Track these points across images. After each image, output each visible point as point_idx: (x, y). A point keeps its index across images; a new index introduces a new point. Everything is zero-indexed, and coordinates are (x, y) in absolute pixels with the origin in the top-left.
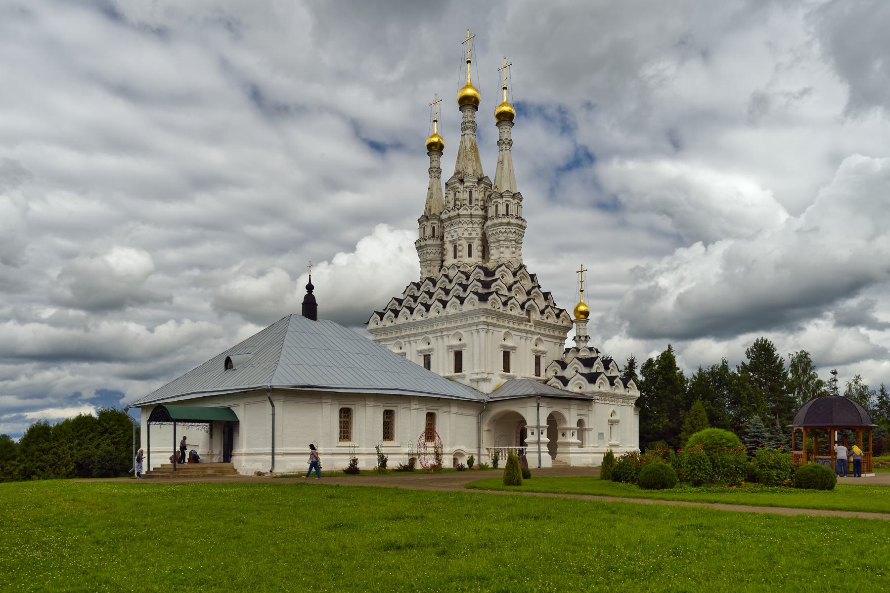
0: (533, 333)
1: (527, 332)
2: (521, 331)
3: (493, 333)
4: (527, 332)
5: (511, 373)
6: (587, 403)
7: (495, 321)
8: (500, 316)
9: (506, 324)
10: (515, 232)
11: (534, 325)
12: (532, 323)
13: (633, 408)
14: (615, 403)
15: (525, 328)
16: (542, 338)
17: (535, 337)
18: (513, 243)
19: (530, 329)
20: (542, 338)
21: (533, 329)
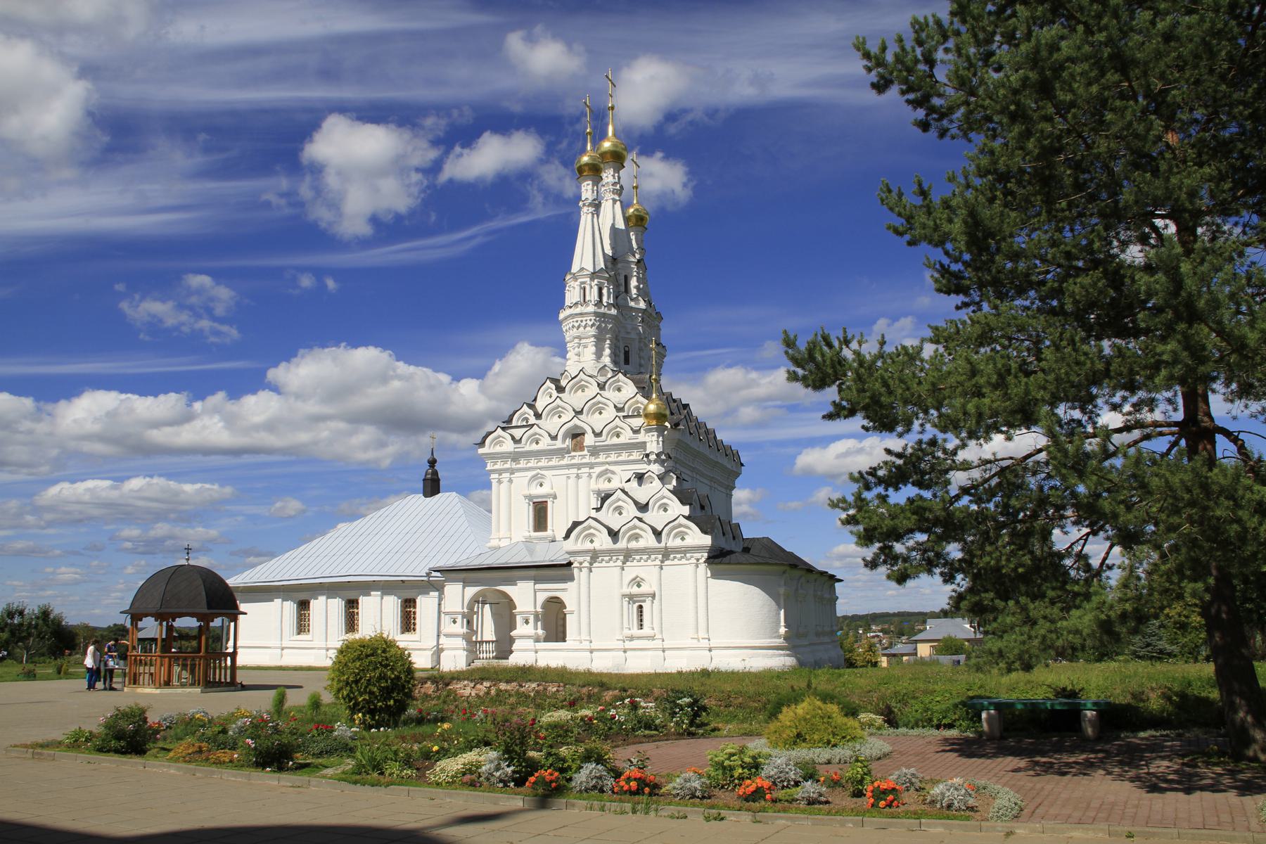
0: (591, 466)
1: (579, 466)
2: (569, 466)
3: (510, 481)
4: (579, 466)
5: (549, 533)
7: (507, 466)
8: (515, 457)
9: (532, 463)
10: (573, 326)
12: (585, 452)
13: (703, 567)
14: (642, 563)
16: (611, 468)
17: (598, 470)
18: (576, 341)
19: (584, 461)
20: (611, 468)
21: (586, 460)
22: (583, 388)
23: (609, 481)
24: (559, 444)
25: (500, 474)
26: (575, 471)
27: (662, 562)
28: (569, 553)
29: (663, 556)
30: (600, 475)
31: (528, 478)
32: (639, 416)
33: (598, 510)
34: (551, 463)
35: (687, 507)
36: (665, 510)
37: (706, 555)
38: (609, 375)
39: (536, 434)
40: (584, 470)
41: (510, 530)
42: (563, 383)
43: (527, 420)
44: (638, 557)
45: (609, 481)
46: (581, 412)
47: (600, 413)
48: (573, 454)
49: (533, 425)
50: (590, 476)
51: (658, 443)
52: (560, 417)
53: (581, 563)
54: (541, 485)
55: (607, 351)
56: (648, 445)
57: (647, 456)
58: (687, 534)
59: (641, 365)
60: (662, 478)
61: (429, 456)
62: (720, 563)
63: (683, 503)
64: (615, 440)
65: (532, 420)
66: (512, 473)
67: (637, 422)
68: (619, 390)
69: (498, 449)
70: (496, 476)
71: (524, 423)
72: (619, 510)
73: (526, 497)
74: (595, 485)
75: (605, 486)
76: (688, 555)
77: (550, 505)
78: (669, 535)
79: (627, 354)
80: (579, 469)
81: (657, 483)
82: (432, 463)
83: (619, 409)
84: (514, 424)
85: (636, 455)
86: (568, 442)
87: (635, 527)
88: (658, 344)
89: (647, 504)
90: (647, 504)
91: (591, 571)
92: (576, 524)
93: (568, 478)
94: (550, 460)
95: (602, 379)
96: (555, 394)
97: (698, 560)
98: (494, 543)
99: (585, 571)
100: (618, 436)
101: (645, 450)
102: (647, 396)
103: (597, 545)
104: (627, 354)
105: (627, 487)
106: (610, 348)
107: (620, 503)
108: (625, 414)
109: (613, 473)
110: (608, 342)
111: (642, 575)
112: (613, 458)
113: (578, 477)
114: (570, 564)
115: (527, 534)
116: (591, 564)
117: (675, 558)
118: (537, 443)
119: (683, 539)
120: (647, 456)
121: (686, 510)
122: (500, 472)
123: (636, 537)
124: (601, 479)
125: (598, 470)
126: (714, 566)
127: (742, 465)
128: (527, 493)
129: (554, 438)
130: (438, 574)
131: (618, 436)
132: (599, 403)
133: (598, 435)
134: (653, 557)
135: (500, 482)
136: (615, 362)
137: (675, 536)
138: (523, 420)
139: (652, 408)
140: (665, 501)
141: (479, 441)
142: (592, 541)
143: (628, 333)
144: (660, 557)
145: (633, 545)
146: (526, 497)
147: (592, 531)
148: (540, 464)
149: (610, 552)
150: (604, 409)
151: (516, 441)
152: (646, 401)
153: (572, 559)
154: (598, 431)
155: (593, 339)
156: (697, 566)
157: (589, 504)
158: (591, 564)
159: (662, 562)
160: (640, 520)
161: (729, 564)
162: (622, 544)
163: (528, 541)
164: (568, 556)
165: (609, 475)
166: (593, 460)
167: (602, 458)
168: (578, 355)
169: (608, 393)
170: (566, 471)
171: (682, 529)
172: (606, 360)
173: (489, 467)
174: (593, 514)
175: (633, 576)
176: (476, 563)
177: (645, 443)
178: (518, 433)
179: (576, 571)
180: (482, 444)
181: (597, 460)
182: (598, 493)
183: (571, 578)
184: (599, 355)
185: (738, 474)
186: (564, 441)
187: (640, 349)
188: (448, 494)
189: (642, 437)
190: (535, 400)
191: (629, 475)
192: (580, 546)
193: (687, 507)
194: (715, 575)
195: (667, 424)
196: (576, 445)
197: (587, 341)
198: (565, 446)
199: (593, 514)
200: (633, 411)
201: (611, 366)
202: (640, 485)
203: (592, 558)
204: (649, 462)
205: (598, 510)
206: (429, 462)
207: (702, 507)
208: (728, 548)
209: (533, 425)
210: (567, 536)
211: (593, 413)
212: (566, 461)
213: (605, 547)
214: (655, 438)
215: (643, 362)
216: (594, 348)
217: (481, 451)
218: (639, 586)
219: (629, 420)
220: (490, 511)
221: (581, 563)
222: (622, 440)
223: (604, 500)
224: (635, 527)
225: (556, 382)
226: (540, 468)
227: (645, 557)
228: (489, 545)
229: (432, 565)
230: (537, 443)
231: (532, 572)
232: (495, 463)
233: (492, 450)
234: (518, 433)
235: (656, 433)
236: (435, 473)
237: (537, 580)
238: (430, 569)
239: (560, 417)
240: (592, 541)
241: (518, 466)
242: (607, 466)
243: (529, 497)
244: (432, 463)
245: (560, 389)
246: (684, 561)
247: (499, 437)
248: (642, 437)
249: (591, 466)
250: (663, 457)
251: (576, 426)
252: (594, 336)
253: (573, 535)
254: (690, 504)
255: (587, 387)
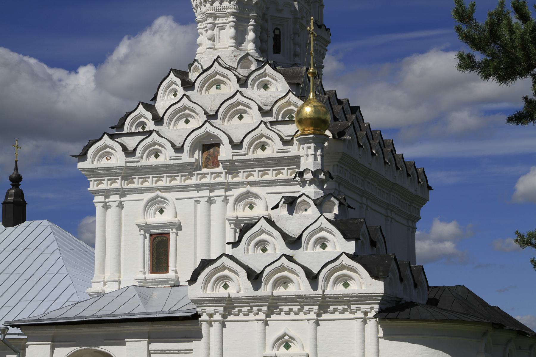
0: (228, 187)
1: (211, 187)
3: (121, 206)
4: (211, 187)
5: (171, 274)
6: (188, 327)
11: (224, 171)
12: (220, 169)
13: (372, 324)
14: (292, 316)
15: (204, 181)
16: (254, 190)
17: (236, 192)
18: (210, 20)
19: (219, 180)
20: (254, 190)
22: (218, 84)
23: (251, 207)
24: (185, 158)
25: (107, 197)
26: (206, 193)
27: (319, 315)
28: (195, 301)
29: (320, 308)
30: (239, 200)
31: (143, 203)
32: (291, 121)
33: (235, 244)
34: (174, 183)
35: (352, 244)
36: (324, 246)
37: (377, 307)
38: (253, 68)
39: (155, 144)
40: (217, 192)
41: (119, 270)
42: (192, 76)
43: (143, 125)
44: (286, 308)
45: (251, 207)
46: (214, 116)
47: (241, 118)
48: (204, 171)
49: (150, 133)
50: (226, 200)
51: (315, 158)
52: (187, 122)
53: (211, 316)
54: (161, 211)
55: (251, 35)
56: (302, 160)
57: (301, 174)
58: (351, 278)
59: (295, 55)
60: (320, 204)
61: (11, 171)
62: (396, 319)
63: (347, 237)
64: (260, 154)
65: (150, 125)
66: (123, 195)
67: (289, 130)
68: (266, 87)
69: (104, 163)
70: (101, 199)
71: (140, 130)
72: (263, 246)
73: (140, 227)
74: (230, 213)
75: (244, 213)
76: (353, 307)
77: (172, 237)
78: (327, 279)
79: (277, 39)
80: (211, 191)
81: (313, 211)
82: (16, 180)
83: (264, 113)
84: (126, 130)
85: (286, 174)
86: (197, 155)
87: (283, 268)
88: (319, 26)
89: (300, 237)
90: (300, 237)
91: (223, 325)
92: (205, 263)
93: (197, 202)
94: (174, 178)
95: (243, 72)
96: (181, 91)
97: (366, 313)
98: (97, 288)
99: (216, 325)
100: (263, 148)
101: (299, 166)
102: (303, 96)
103: (232, 291)
104: (277, 39)
105: (274, 215)
106: (254, 31)
107: (264, 236)
108: (273, 119)
109: (256, 196)
110: (252, 22)
111: (292, 333)
112: (256, 176)
113: (210, 201)
114: (196, 316)
115: (142, 276)
116: (224, 316)
117: (335, 310)
118: (157, 156)
119: (346, 285)
120: (301, 174)
121: (351, 247)
122: (107, 193)
123: (285, 282)
124: (241, 205)
125: (236, 192)
126: (387, 322)
127: (430, 188)
128: (142, 221)
129: (179, 149)
130: (18, 330)
131: (263, 148)
132: (239, 103)
133: (236, 146)
134: (306, 308)
135: (106, 207)
136: (260, 49)
137: (336, 282)
138: (138, 126)
139: (308, 110)
140: (323, 234)
141: (79, 152)
142: (226, 287)
143: (280, 11)
144: (316, 308)
145: (281, 291)
146: (140, 227)
147: (226, 272)
148: (160, 184)
149: (249, 301)
150: (245, 112)
151: (129, 153)
152: (300, 102)
153: (199, 310)
154: (236, 140)
155: (231, 18)
156: (365, 322)
157: (224, 236)
158: (224, 316)
159: (319, 315)
160: (290, 258)
161: (408, 319)
162: (266, 290)
163: (143, 285)
164: (193, 306)
165: (252, 199)
166: (230, 179)
167: (241, 177)
168: (212, 39)
169: (251, 92)
170: (195, 194)
171: (345, 272)
172: (250, 46)
173: (92, 187)
174: (229, 250)
175: (280, 333)
176: (71, 314)
177: (298, 158)
178: (131, 142)
179: (204, 326)
180: (83, 156)
181: (236, 180)
182: (236, 222)
183: (199, 336)
184: (239, 39)
185: (424, 201)
186: (192, 154)
187: (295, 33)
188: (36, 222)
189: (294, 150)
190: (155, 98)
191: (276, 199)
192: (210, 293)
193: (352, 244)
194: (389, 335)
195: (328, 133)
196: (207, 159)
197: (224, 20)
198: (193, 160)
199: (229, 250)
200: (283, 116)
201: (256, 55)
202: (291, 212)
203: (225, 308)
204: (303, 183)
205: (235, 244)
206: (11, 179)
207: (373, 244)
208: (407, 299)
209: (150, 133)
210: (193, 280)
211: (231, 117)
212: (193, 181)
213: (242, 294)
214: (311, 151)
215: (298, 49)
216: (233, 31)
217: (81, 165)
218: (287, 347)
219: (278, 127)
220: (93, 246)
221: (211, 316)
222: (269, 153)
223: (243, 231)
224: (283, 268)
225: (182, 75)
226: (161, 189)
227: (295, 308)
228: (90, 290)
229: (10, 318)
230: (157, 156)
231: (146, 328)
232: (101, 182)
233: (95, 165)
234: (131, 142)
235: (312, 145)
236: (20, 194)
237: (152, 338)
238: (6, 324)
239: (187, 122)
240: (226, 287)
241: (131, 186)
242: (249, 188)
243: (145, 228)
244: (16, 180)
245: (188, 85)
246: (347, 315)
247: (106, 147)
248: (294, 150)
249: (228, 187)
250: (322, 176)
251: (208, 135)
252: (234, 14)
253: (201, 278)
254: (357, 240)
255: (223, 82)
